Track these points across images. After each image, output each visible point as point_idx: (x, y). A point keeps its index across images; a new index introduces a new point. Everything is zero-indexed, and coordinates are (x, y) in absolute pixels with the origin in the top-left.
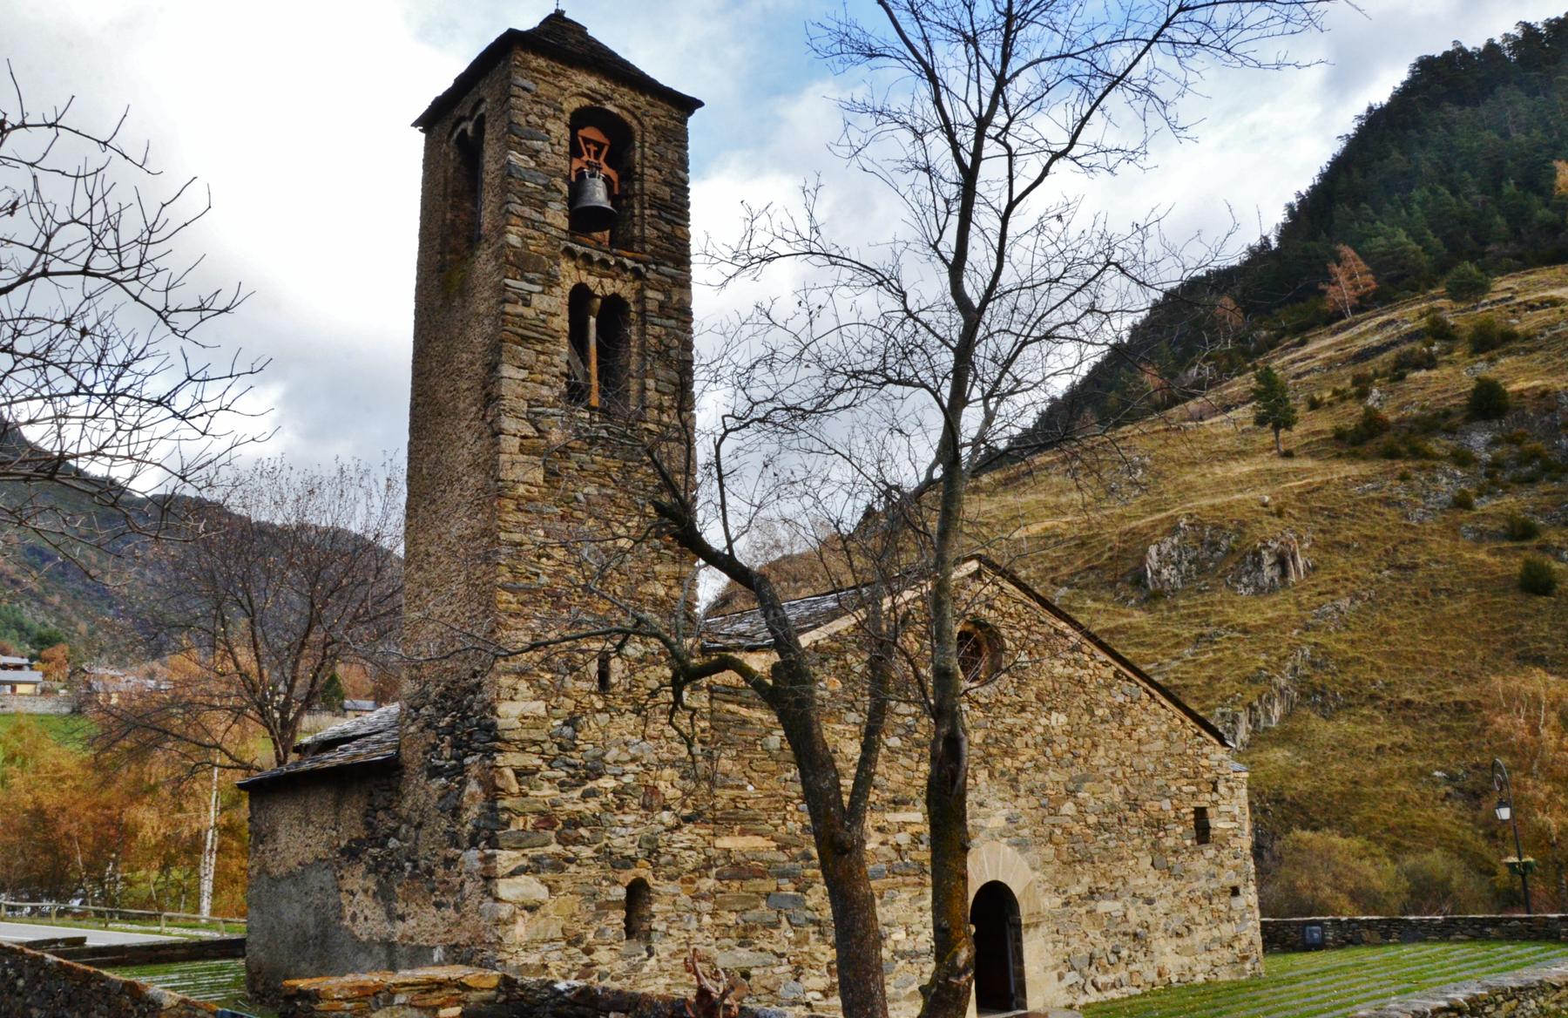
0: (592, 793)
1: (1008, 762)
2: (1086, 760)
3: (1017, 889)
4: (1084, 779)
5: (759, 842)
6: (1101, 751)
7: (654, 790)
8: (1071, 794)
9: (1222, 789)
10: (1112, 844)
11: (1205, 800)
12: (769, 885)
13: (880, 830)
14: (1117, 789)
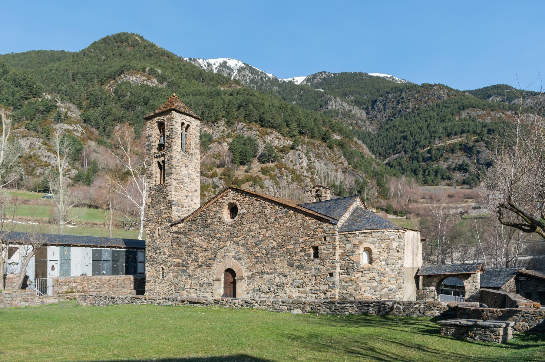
0: (156, 253)
1: (236, 238)
2: (263, 235)
3: (236, 271)
4: (262, 241)
5: (179, 260)
6: (269, 232)
7: (164, 252)
8: (257, 245)
9: (328, 239)
10: (270, 259)
11: (317, 243)
12: (181, 268)
13: (202, 257)
14: (275, 243)
